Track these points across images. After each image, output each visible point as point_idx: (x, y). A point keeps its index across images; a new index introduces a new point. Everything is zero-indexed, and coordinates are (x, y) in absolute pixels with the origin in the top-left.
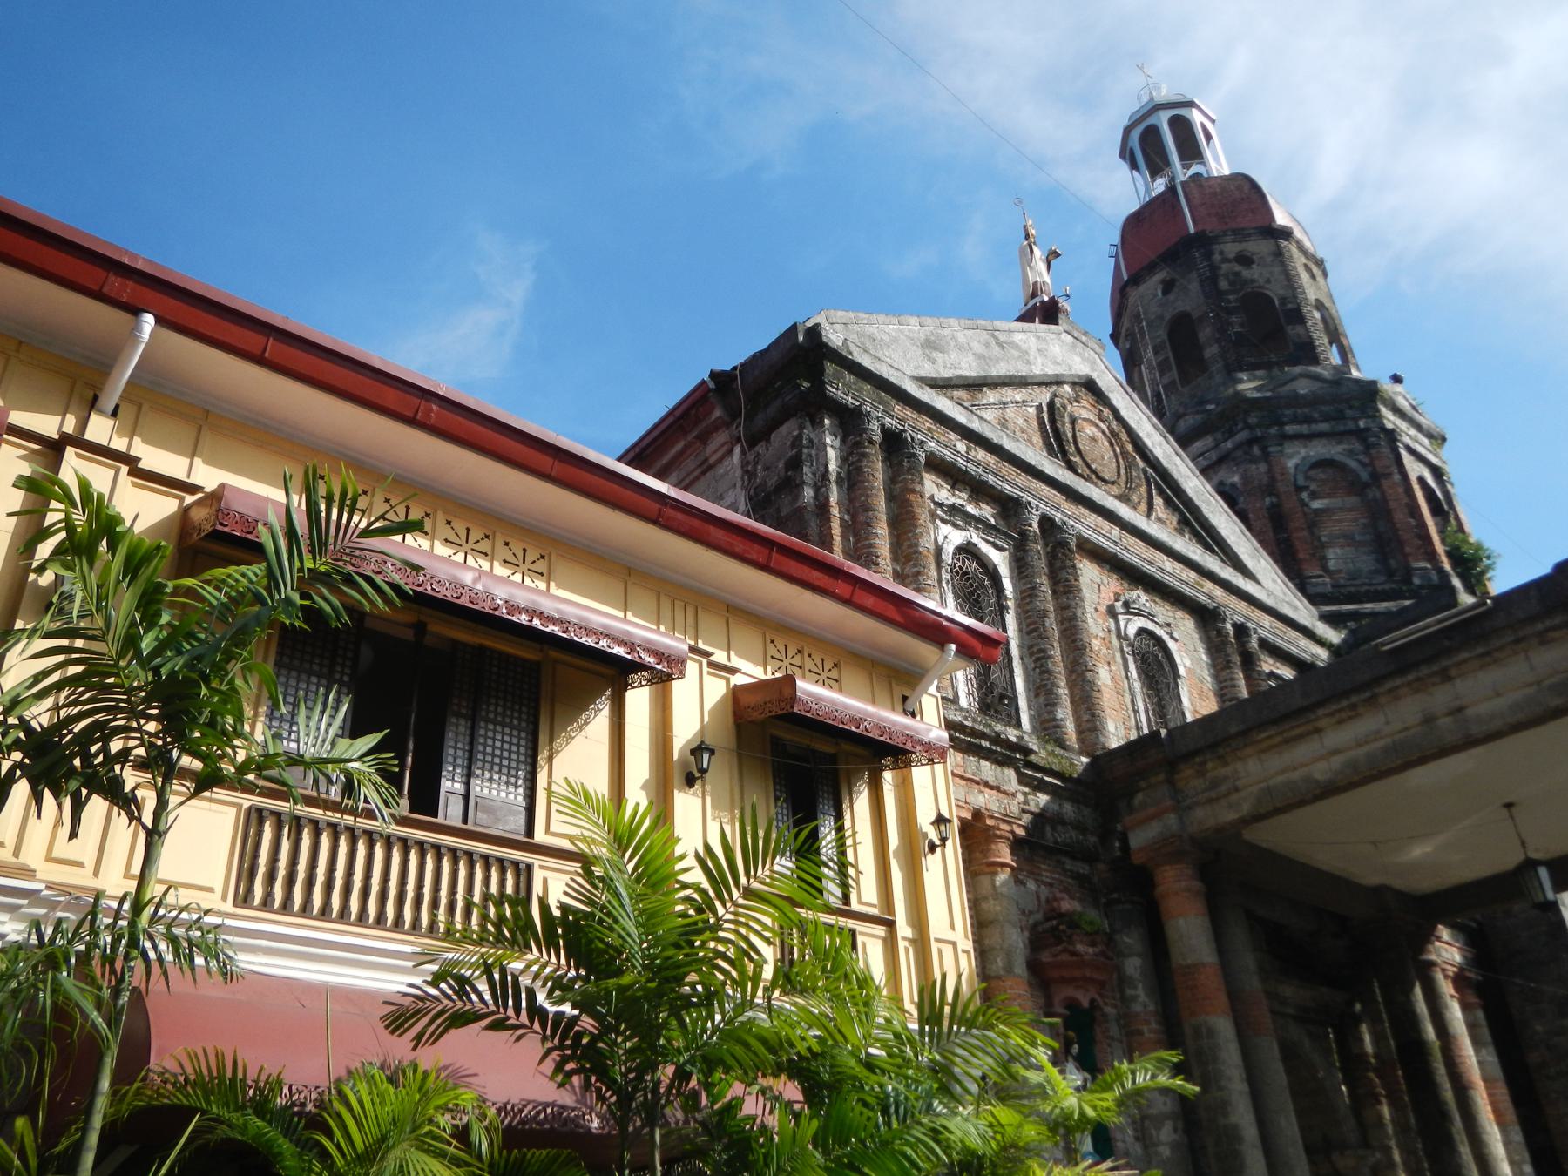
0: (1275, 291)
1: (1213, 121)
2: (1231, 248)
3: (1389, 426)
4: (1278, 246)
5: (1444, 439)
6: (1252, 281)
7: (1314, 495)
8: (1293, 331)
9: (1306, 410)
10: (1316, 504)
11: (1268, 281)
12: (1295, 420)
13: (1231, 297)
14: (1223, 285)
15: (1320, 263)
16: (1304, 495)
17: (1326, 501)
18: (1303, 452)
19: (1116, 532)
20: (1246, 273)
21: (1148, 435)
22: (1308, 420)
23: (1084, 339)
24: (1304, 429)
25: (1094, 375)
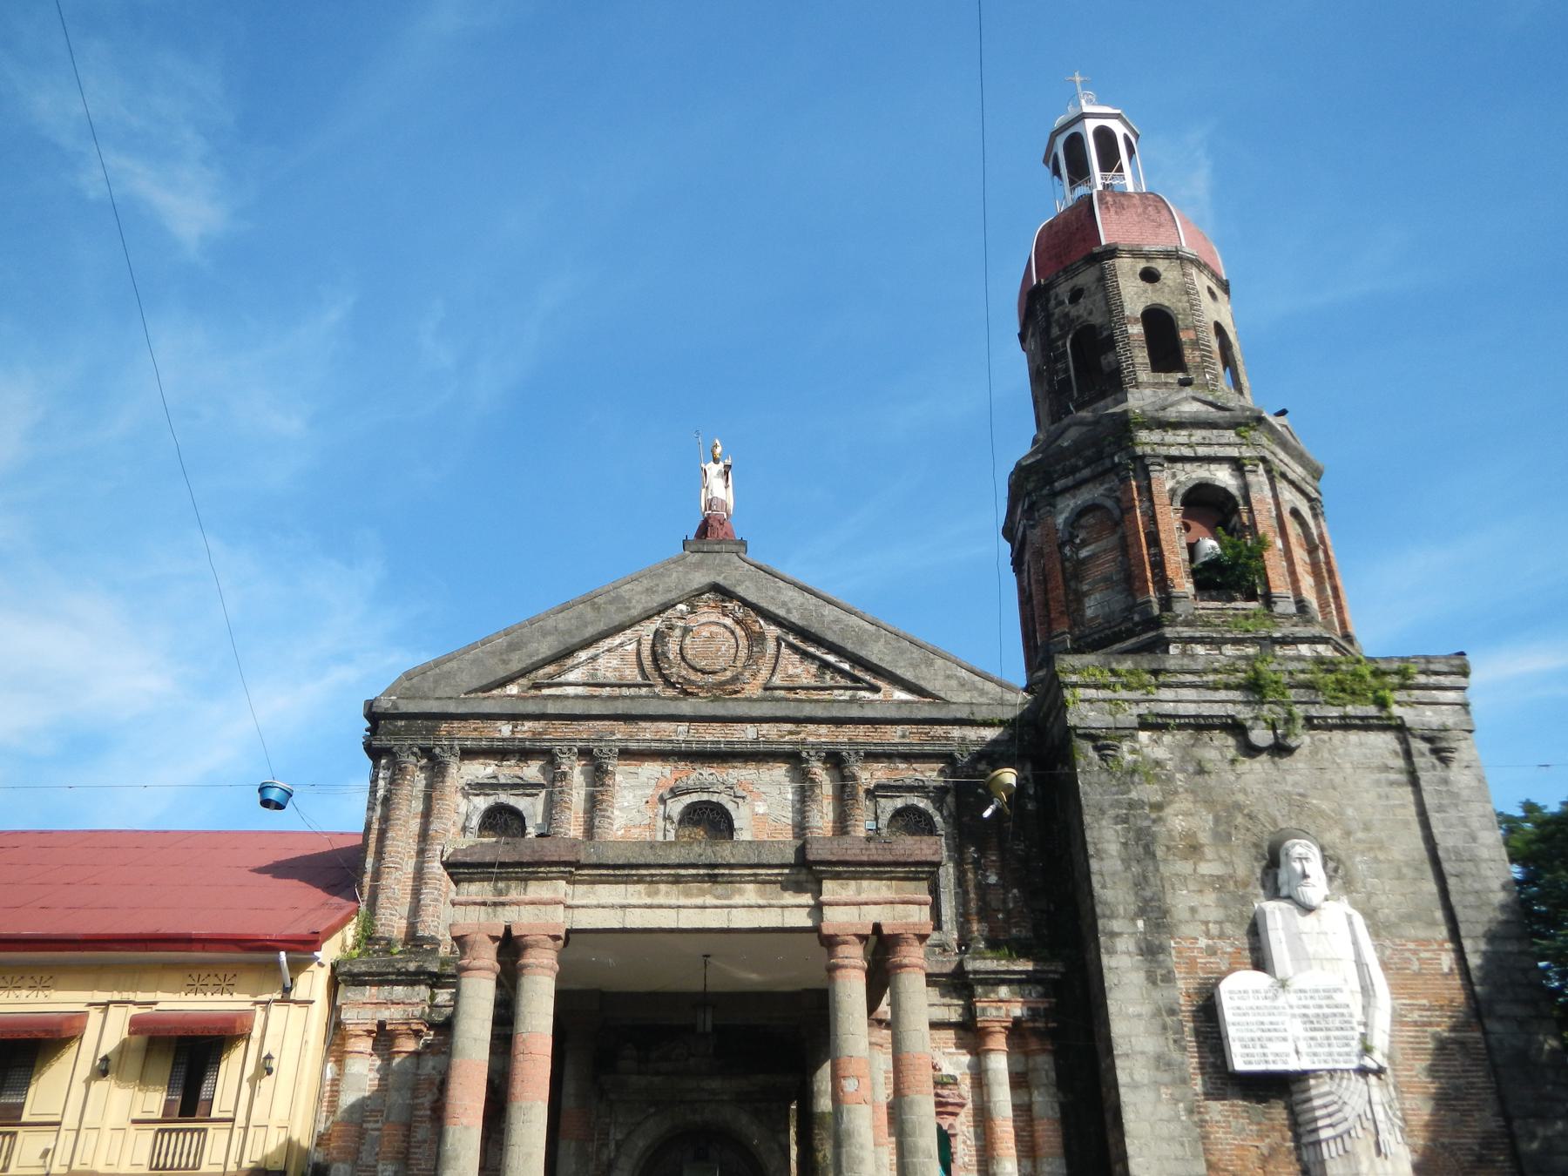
0: (1097, 319)
1: (1117, 116)
2: (1063, 290)
3: (1139, 450)
4: (1103, 269)
5: (1260, 420)
7: (1084, 544)
8: (1107, 360)
10: (1084, 553)
11: (1090, 313)
12: (1065, 474)
14: (1055, 331)
16: (1067, 550)
19: (683, 727)
20: (1074, 311)
21: (784, 604)
22: (1075, 470)
23: (717, 548)
24: (1069, 481)
25: (720, 580)
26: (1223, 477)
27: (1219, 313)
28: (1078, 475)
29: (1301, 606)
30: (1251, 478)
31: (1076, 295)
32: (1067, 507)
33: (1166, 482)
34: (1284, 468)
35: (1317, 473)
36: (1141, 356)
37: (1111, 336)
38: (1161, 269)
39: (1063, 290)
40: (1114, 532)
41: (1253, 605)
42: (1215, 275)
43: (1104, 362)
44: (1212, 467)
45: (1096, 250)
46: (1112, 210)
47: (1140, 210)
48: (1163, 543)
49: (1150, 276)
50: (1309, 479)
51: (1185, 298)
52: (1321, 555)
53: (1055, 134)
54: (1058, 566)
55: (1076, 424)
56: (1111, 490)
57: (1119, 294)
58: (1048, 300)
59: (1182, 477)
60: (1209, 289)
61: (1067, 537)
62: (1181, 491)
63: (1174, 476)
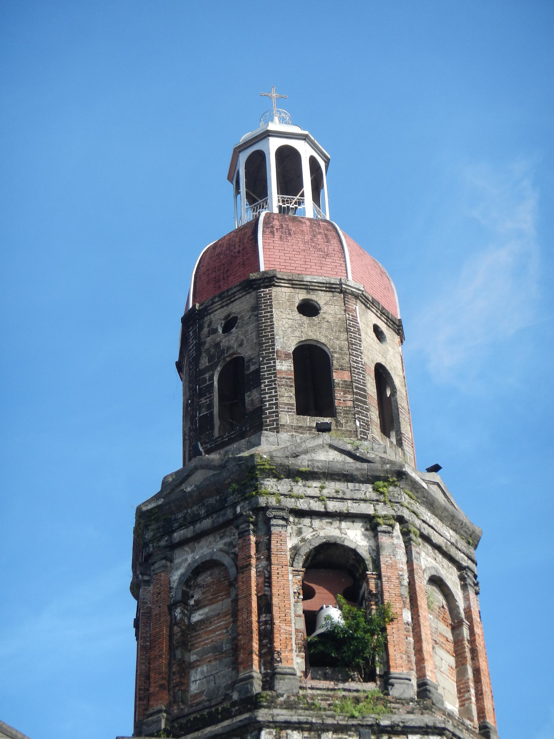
0: (246, 352)
1: (305, 138)
2: (217, 317)
3: (262, 501)
4: (258, 297)
5: (401, 475)
6: (229, 348)
7: (198, 606)
8: (251, 397)
9: (195, 508)
10: (196, 617)
11: (241, 345)
13: (207, 376)
14: (204, 362)
15: (330, 288)
16: (178, 613)
17: (206, 610)
18: (190, 558)
22: (196, 519)
24: (188, 532)
26: (355, 536)
27: (384, 354)
28: (198, 526)
29: (424, 690)
30: (384, 539)
31: (230, 324)
32: (186, 559)
33: (291, 539)
34: (427, 531)
35: (473, 540)
36: (287, 396)
37: (258, 371)
38: (321, 302)
39: (217, 317)
40: (228, 595)
41: (371, 687)
42: (384, 313)
43: (247, 400)
44: (344, 524)
45: (253, 276)
46: (277, 235)
47: (307, 238)
48: (275, 609)
49: (308, 309)
50: (462, 544)
51: (344, 336)
52: (466, 632)
53: (238, 150)
54: (165, 631)
55: (203, 467)
56: (231, 545)
57: (272, 326)
58: (201, 328)
59: (308, 534)
60: (376, 329)
61: (179, 597)
62: (305, 550)
63: (299, 532)
